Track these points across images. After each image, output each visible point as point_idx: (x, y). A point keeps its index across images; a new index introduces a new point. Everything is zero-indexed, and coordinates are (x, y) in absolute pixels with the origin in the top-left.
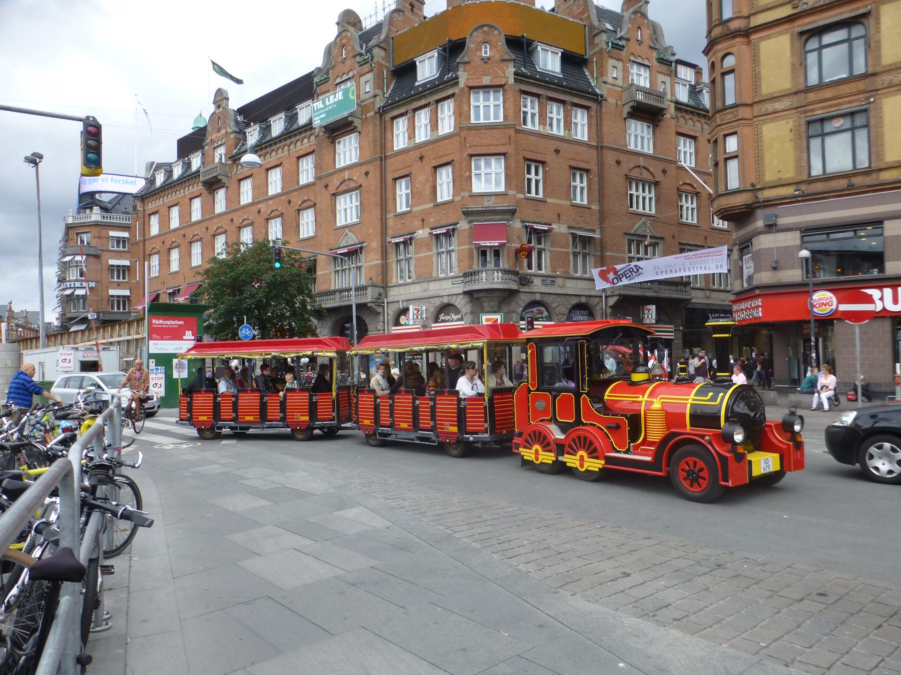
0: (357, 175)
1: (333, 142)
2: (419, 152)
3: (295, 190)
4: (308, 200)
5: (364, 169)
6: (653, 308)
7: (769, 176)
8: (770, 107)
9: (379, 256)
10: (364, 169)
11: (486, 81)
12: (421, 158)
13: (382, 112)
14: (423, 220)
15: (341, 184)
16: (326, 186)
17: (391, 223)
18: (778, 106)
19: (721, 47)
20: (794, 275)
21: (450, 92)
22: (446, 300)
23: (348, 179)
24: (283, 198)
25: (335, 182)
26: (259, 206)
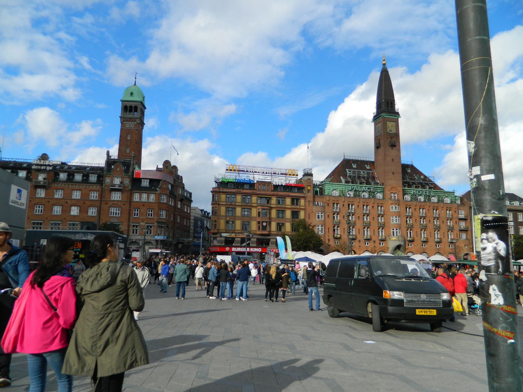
0: (119, 204)
1: (111, 192)
2: (144, 204)
3: (88, 200)
4: (94, 205)
5: (123, 203)
6: (181, 245)
7: (221, 228)
8: (222, 217)
9: (127, 227)
10: (123, 203)
11: (164, 193)
12: (144, 205)
13: (131, 190)
14: (143, 221)
15: (113, 204)
16: (106, 204)
17: (131, 219)
18: (223, 217)
19: (216, 206)
20: (223, 244)
21: (155, 192)
22: (148, 241)
23: (116, 204)
24: (81, 201)
25: (111, 203)
26: (67, 201)
